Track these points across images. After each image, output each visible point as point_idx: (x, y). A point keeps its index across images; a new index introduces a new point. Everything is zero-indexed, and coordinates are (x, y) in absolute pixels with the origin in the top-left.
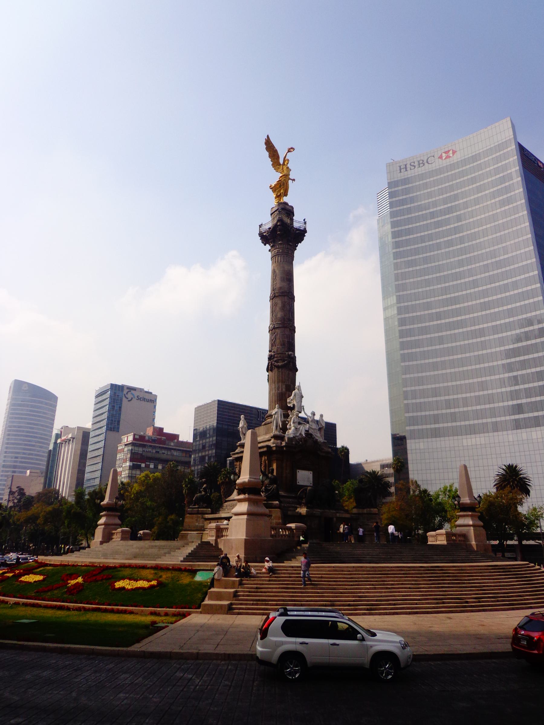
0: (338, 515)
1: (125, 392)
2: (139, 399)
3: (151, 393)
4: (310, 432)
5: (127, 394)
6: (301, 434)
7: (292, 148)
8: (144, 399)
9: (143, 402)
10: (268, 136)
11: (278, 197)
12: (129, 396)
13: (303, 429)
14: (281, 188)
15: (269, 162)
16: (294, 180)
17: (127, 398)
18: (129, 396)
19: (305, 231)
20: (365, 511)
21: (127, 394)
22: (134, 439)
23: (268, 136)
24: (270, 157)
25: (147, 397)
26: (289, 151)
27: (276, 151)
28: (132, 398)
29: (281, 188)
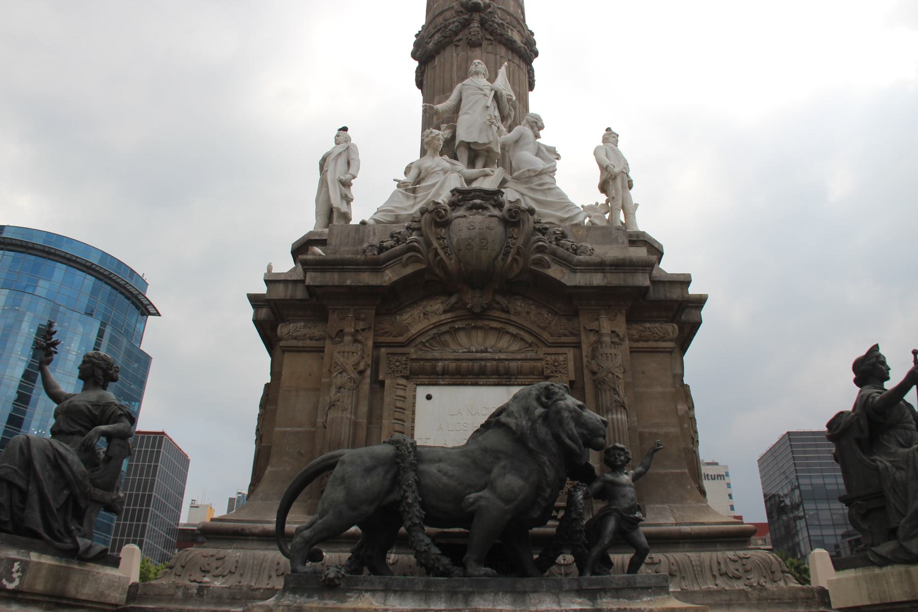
3: (716, 464)
4: (510, 195)
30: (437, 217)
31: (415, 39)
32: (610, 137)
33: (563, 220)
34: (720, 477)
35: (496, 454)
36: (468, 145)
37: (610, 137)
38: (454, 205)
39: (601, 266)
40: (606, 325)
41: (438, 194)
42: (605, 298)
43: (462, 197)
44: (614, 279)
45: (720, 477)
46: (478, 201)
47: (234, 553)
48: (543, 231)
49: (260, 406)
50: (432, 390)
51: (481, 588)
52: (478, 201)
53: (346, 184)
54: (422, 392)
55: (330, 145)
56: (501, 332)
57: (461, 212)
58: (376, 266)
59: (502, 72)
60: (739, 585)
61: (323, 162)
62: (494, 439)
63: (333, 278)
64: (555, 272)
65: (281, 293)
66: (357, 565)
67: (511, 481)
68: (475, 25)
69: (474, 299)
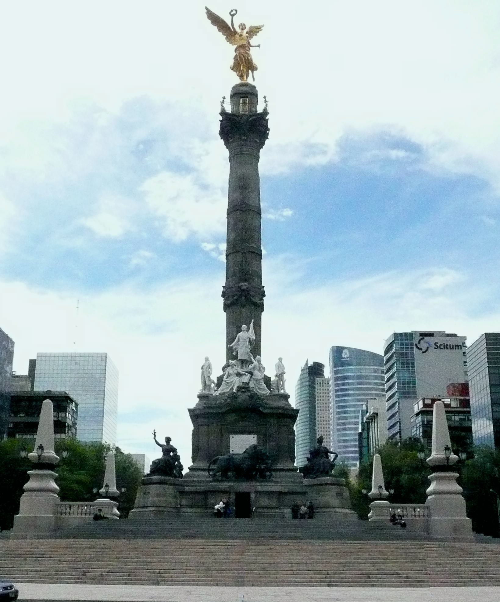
0: (259, 488)
1: (415, 341)
2: (437, 347)
4: (252, 385)
5: (419, 343)
6: (232, 389)
7: (232, 11)
8: (446, 346)
9: (445, 351)
10: (207, 9)
11: (241, 77)
12: (424, 346)
13: (237, 382)
14: (244, 64)
15: (221, 37)
16: (259, 46)
17: (421, 349)
18: (424, 346)
19: (265, 113)
20: (315, 481)
21: (419, 343)
22: (425, 405)
23: (207, 9)
24: (219, 30)
25: (451, 342)
26: (233, 16)
27: (223, 22)
28: (428, 348)
29: (244, 64)
30: (234, 396)
31: (222, 289)
32: (280, 359)
33: (263, 394)
34: (458, 347)
35: (245, 458)
36: (241, 360)
37: (280, 359)
38: (238, 391)
39: (272, 408)
40: (272, 420)
41: (234, 386)
42: (271, 415)
43: (239, 388)
44: (275, 411)
45: (458, 347)
46: (243, 390)
47: (196, 473)
48: (259, 398)
49: (193, 435)
50: (233, 435)
51: (244, 481)
52: (243, 390)
53: (209, 377)
54: (231, 436)
55: (203, 362)
56: (249, 421)
57: (239, 393)
58: (220, 408)
59: (252, 325)
60: (292, 480)
61: (202, 368)
62: (246, 455)
63: (211, 411)
64: (261, 409)
65: (197, 412)
66: (222, 476)
67: (248, 462)
68: (244, 298)
69: (243, 415)
